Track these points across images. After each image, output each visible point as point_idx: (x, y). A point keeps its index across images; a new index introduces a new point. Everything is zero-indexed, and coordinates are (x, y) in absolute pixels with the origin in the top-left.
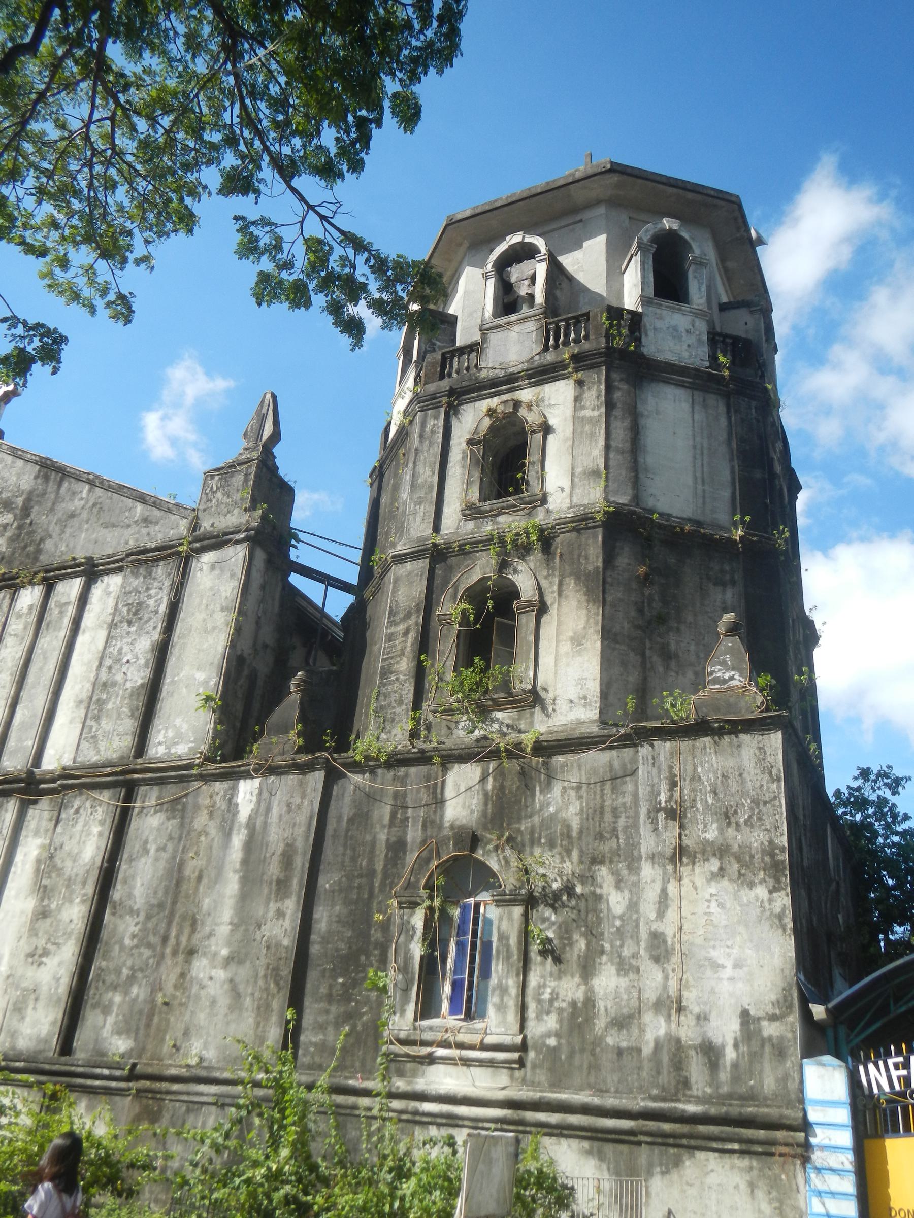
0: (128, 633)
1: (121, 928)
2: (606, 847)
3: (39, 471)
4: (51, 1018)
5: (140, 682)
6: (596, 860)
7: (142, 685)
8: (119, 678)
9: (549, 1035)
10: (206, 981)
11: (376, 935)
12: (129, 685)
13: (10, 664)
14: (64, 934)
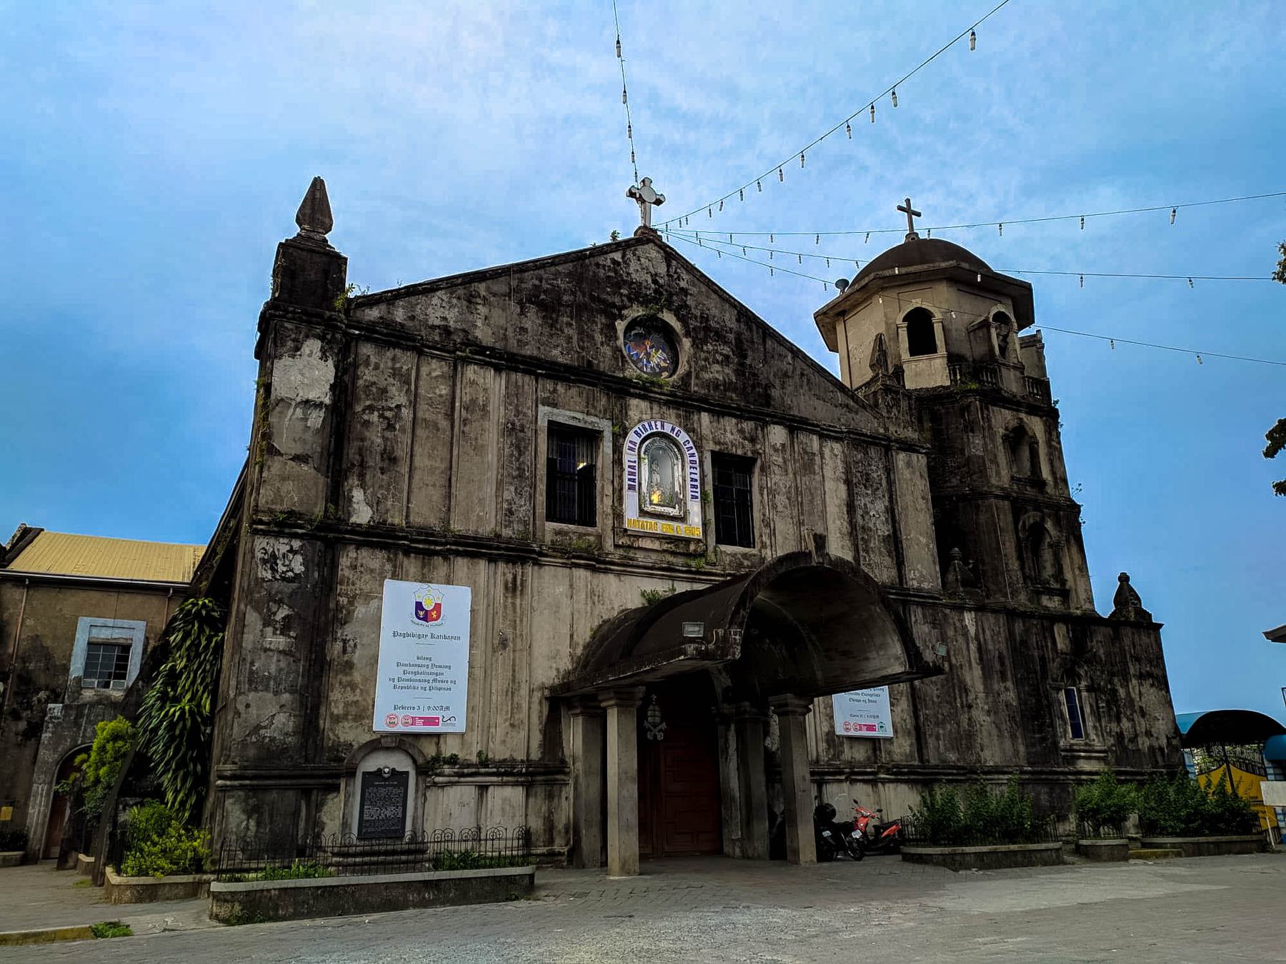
1: (929, 691)
2: (1115, 669)
3: (739, 316)
4: (908, 742)
5: (887, 533)
6: (1112, 674)
7: (889, 535)
8: (871, 525)
9: (1113, 745)
10: (982, 723)
14: (898, 693)
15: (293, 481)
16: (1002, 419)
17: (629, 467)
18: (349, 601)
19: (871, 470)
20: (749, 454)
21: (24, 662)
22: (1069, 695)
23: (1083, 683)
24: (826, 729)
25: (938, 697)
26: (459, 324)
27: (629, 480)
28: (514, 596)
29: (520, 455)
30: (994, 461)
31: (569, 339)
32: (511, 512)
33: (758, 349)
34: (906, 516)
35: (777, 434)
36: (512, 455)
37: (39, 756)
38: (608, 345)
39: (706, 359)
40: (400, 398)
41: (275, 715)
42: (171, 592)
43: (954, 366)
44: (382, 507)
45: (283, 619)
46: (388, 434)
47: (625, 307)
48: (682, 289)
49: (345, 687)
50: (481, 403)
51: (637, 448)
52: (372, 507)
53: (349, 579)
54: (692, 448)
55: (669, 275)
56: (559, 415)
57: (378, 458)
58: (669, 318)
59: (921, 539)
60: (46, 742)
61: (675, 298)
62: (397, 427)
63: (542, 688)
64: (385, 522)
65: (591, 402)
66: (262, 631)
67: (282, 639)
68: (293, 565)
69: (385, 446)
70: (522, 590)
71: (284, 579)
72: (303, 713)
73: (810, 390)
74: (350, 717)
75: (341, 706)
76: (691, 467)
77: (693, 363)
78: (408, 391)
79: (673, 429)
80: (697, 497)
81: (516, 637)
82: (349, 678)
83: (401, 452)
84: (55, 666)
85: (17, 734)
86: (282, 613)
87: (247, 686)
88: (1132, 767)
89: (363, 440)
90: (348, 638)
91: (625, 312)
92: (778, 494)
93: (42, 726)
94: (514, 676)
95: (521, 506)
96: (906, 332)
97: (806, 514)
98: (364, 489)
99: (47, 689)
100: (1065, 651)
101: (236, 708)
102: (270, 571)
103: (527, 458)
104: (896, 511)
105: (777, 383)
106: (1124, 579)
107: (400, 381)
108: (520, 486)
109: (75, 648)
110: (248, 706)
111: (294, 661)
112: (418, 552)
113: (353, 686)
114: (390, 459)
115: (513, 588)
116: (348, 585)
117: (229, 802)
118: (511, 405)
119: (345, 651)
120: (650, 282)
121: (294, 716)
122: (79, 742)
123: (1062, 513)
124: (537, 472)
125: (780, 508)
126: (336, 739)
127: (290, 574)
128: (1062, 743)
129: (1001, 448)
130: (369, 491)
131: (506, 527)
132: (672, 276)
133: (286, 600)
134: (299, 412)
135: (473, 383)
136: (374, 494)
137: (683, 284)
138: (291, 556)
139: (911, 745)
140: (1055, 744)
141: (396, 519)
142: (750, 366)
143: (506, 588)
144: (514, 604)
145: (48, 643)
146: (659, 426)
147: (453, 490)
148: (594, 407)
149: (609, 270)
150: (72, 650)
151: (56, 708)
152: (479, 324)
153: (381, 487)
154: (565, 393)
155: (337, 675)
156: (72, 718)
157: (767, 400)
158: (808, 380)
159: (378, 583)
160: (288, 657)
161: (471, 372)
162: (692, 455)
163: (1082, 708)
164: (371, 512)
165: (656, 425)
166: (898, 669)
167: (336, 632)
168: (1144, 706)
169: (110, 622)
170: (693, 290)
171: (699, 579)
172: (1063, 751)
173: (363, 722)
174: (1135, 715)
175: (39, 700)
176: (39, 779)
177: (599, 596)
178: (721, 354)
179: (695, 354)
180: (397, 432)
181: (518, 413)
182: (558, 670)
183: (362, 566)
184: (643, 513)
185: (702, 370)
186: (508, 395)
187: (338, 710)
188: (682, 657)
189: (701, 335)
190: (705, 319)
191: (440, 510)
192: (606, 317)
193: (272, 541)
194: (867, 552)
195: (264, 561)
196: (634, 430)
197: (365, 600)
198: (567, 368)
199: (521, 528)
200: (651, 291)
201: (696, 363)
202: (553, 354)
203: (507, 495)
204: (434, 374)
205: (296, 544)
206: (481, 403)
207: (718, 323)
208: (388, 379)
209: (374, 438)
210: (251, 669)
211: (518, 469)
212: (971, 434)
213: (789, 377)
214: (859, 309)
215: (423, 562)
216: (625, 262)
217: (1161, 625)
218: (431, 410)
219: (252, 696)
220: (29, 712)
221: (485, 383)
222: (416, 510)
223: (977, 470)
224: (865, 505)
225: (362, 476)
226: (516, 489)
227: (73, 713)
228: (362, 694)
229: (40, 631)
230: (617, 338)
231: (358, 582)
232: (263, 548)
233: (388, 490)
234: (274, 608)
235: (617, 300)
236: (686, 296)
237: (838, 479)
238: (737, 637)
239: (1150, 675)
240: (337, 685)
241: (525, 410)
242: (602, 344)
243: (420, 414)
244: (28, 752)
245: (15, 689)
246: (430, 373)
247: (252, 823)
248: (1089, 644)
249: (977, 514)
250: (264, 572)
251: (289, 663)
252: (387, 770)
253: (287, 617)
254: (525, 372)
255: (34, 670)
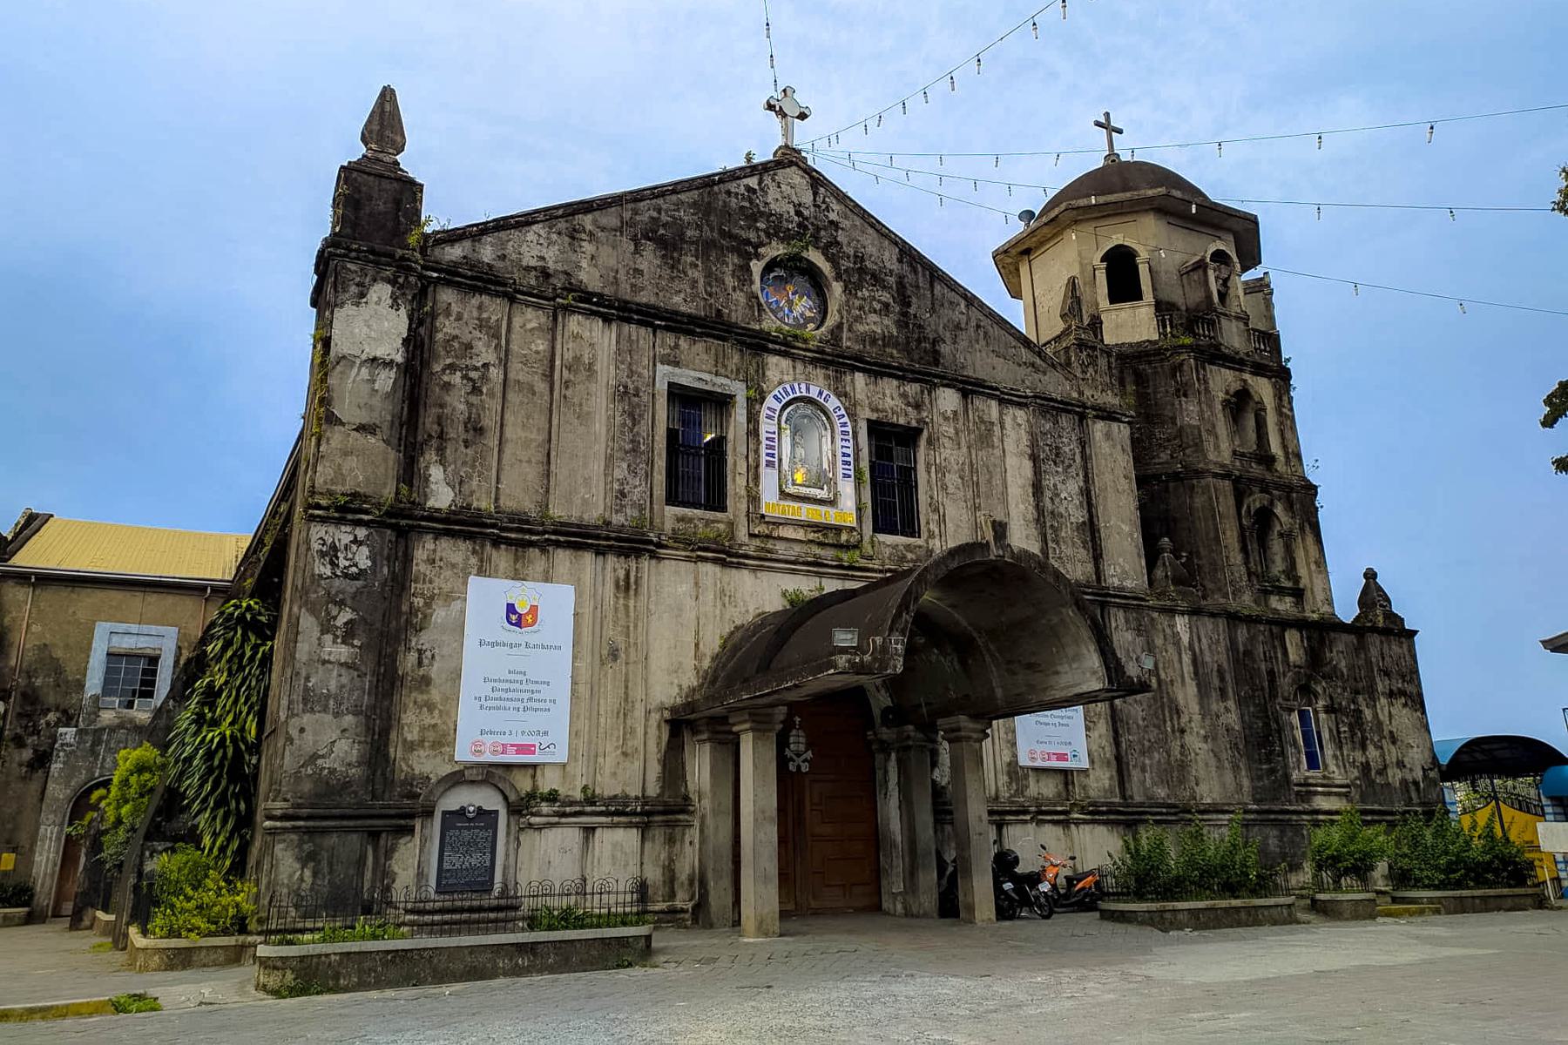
0: (1057, 472)
1: (1133, 712)
2: (1360, 685)
5: (1081, 520)
6: (1357, 692)
7: (1084, 523)
8: (1062, 510)
9: (1357, 778)
11: (1274, 726)
12: (1073, 519)
13: (956, 467)
15: (357, 456)
16: (1222, 381)
17: (767, 439)
18: (426, 603)
19: (1062, 442)
20: (914, 424)
21: (30, 677)
22: (1303, 716)
23: (1321, 703)
24: (1007, 759)
25: (1144, 719)
26: (560, 264)
27: (768, 455)
28: (627, 597)
29: (634, 425)
30: (1212, 431)
31: (694, 283)
32: (623, 494)
33: (924, 295)
34: (1105, 498)
35: (948, 399)
36: (624, 425)
37: (47, 791)
38: (742, 290)
39: (861, 308)
40: (488, 356)
41: (335, 741)
42: (209, 591)
43: (1163, 316)
44: (465, 489)
45: (346, 624)
46: (474, 399)
47: (762, 244)
48: (832, 222)
49: (421, 708)
50: (587, 362)
51: (776, 416)
52: (453, 488)
53: (425, 575)
54: (843, 416)
55: (815, 206)
56: (682, 376)
57: (461, 428)
58: (815, 257)
59: (1123, 527)
60: (56, 775)
61: (823, 233)
62: (485, 390)
63: (661, 708)
64: (469, 507)
65: (720, 360)
66: (319, 639)
67: (344, 649)
68: (357, 558)
69: (470, 414)
70: (636, 589)
71: (346, 576)
72: (369, 740)
73: (987, 345)
74: (427, 744)
75: (416, 731)
76: (842, 440)
77: (845, 313)
78: (498, 346)
79: (820, 393)
80: (849, 476)
81: (629, 646)
82: (425, 697)
83: (489, 421)
84: (68, 682)
85: (21, 765)
86: (345, 616)
87: (301, 706)
88: (1380, 805)
89: (442, 406)
90: (424, 648)
91: (762, 250)
92: (949, 472)
93: (51, 754)
94: (626, 693)
95: (635, 487)
96: (1105, 275)
97: (983, 496)
98: (444, 466)
99: (57, 709)
100: (1298, 663)
101: (287, 732)
102: (329, 566)
103: (643, 428)
104: (1093, 493)
105: (948, 336)
106: (1370, 575)
107: (487, 334)
108: (635, 463)
109: (91, 660)
110: (302, 730)
111: (359, 676)
112: (510, 542)
113: (431, 707)
114: (475, 429)
115: (626, 586)
116: (424, 582)
117: (279, 847)
118: (622, 363)
119: (420, 663)
120: (792, 213)
121: (359, 742)
122: (97, 775)
123: (1294, 495)
124: (655, 446)
125: (951, 489)
126: (409, 770)
127: (354, 569)
128: (1295, 776)
129: (1220, 416)
130: (450, 469)
131: (617, 512)
132: (819, 207)
133: (349, 602)
134: (365, 372)
135: (576, 337)
136: (456, 472)
137: (833, 216)
138: (354, 547)
139: (1111, 778)
140: (1287, 776)
141: (484, 503)
142: (915, 316)
143: (617, 586)
144: (626, 607)
145: (58, 653)
146: (804, 389)
147: (553, 467)
148: (725, 366)
149: (743, 199)
150: (88, 662)
151: (68, 734)
152: (584, 264)
153: (465, 463)
154: (689, 349)
155: (411, 692)
156: (88, 745)
157: (936, 357)
158: (986, 333)
159: (461, 580)
160: (351, 671)
161: (574, 323)
162: (844, 425)
163: (1319, 733)
164: (453, 495)
165: (800, 388)
166: (1095, 685)
167: (410, 640)
168: (1395, 730)
169: (134, 628)
170: (845, 223)
171: (853, 576)
172: (1296, 785)
173: (443, 750)
174: (1384, 741)
175: (48, 724)
176: (47, 819)
177: (730, 596)
178: (879, 301)
179: (848, 301)
180: (484, 397)
181: (631, 373)
182: (680, 686)
183: (441, 560)
184: (784, 495)
185: (856, 321)
186: (619, 351)
187: (412, 735)
188: (832, 671)
189: (855, 278)
190: (859, 258)
191: (537, 491)
192: (740, 256)
193: (332, 529)
194: (1058, 543)
195: (322, 554)
196: (773, 394)
197: (446, 600)
198: (692, 319)
199: (636, 514)
200: (794, 225)
201: (849, 312)
202: (674, 301)
203: (618, 474)
204: (529, 326)
205: (361, 533)
206: (587, 362)
207: (876, 264)
208: (474, 331)
209: (456, 404)
210: (306, 686)
211: (632, 441)
212: (1183, 399)
213: (961, 329)
214: (1048, 246)
215: (516, 555)
216: (762, 189)
217: (1415, 632)
218: (526, 369)
219: (307, 719)
220: (36, 738)
221: (591, 338)
222: (508, 491)
223: (1191, 443)
224: (1055, 485)
225: (441, 451)
226: (629, 466)
227: (89, 738)
228: (441, 716)
229: (48, 639)
230: (752, 282)
231: (436, 579)
232: (321, 538)
233: (473, 467)
234: (334, 611)
235: (752, 236)
236: (836, 231)
237: (1021, 454)
238: (899, 647)
239: (1402, 693)
240: (411, 705)
241: (640, 370)
242: (734, 289)
243: (512, 375)
244: (34, 787)
245: (18, 710)
246: (525, 325)
247: (308, 873)
248: (1328, 655)
249: (1191, 497)
250: (322, 568)
251: (353, 678)
252: (471, 809)
253: (350, 622)
254: (640, 323)
255: (41, 687)
